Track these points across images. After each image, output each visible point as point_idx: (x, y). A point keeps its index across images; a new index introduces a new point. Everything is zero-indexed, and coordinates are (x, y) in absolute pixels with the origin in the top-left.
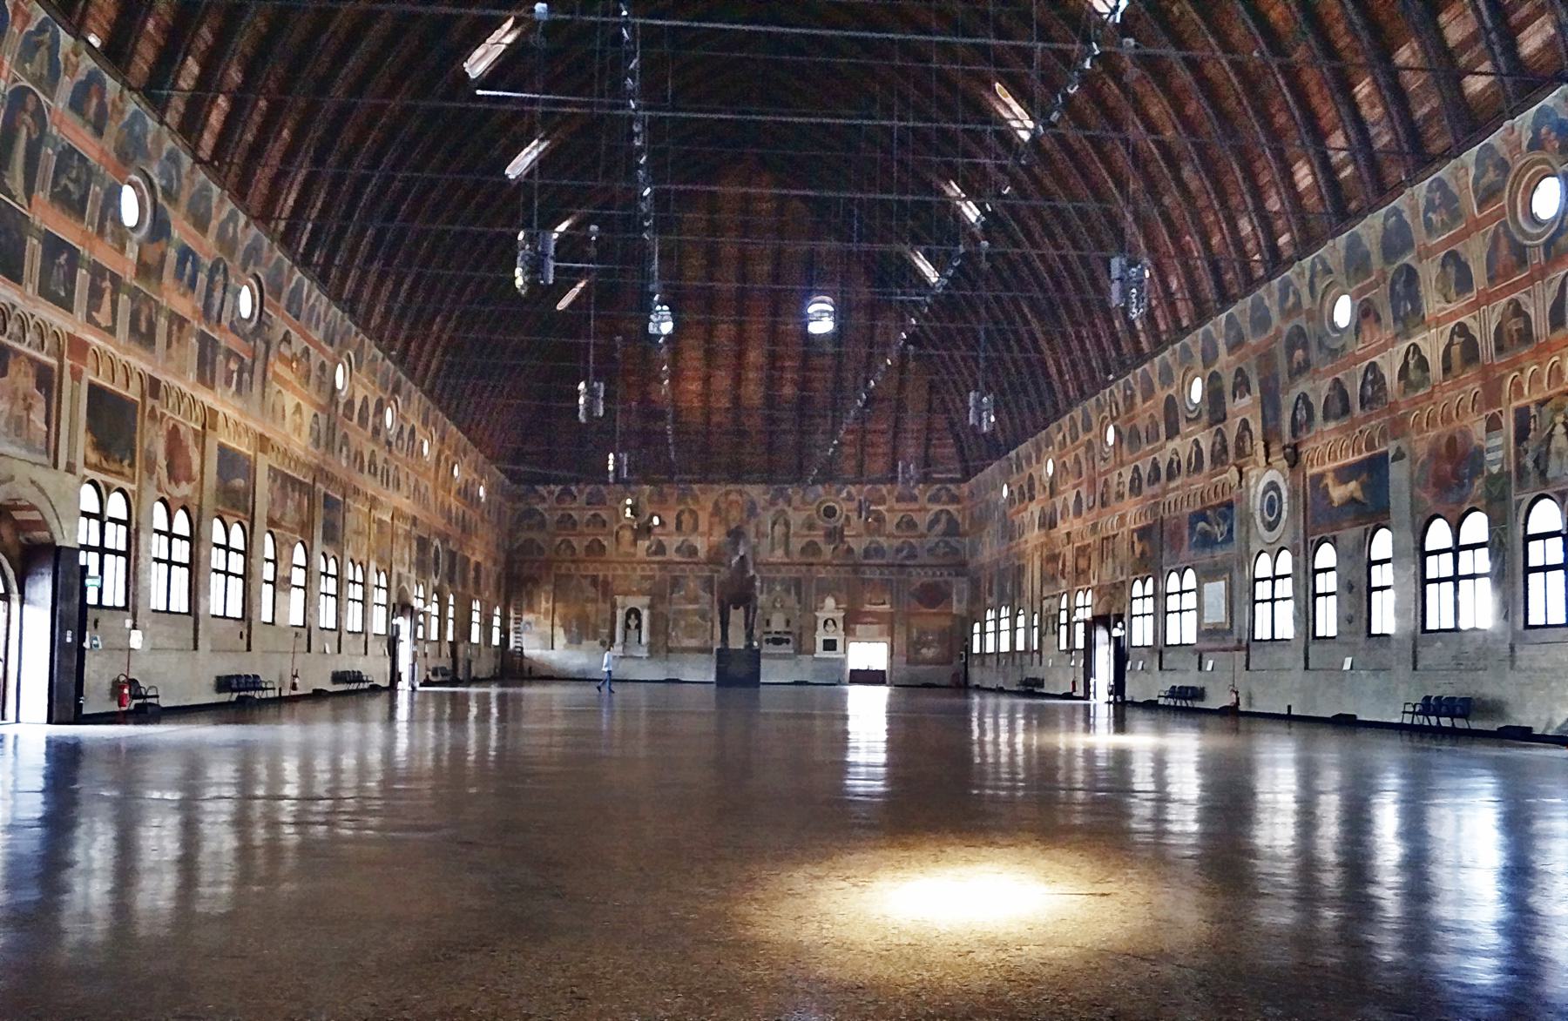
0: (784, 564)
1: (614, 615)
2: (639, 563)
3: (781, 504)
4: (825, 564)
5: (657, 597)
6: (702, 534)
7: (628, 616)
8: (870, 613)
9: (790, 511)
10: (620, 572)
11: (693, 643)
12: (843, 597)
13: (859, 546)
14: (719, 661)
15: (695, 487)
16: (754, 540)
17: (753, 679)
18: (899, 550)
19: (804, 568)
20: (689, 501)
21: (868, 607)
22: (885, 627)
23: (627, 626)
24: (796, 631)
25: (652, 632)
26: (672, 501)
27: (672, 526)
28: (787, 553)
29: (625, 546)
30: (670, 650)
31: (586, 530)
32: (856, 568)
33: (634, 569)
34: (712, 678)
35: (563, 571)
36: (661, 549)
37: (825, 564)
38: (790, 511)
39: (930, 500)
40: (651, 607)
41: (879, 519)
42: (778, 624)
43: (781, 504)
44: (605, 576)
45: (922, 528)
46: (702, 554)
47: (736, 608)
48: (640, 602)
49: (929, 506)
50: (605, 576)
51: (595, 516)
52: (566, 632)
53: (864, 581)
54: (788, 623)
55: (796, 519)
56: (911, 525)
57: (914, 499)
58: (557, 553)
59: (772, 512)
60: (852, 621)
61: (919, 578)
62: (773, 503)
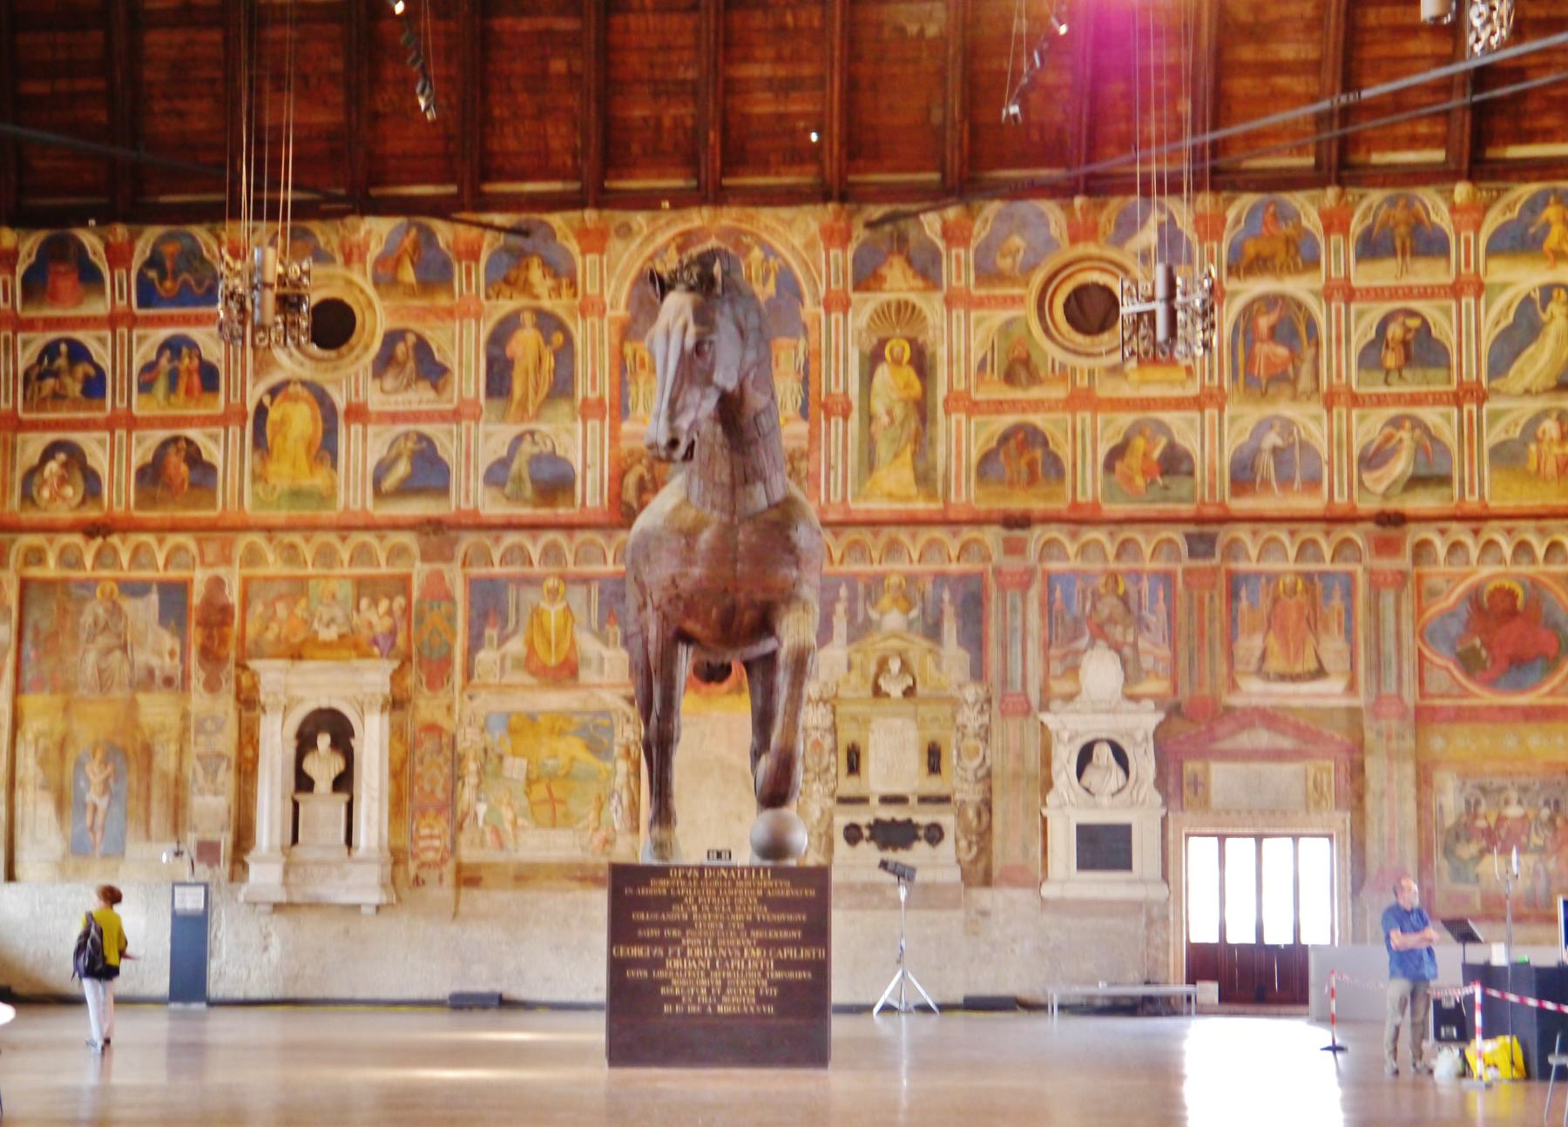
0: (913, 522)
1: (248, 739)
2: (344, 529)
3: (898, 282)
4: (1080, 518)
5: (420, 663)
6: (590, 410)
7: (305, 742)
8: (1269, 718)
9: (932, 307)
10: (273, 565)
11: (560, 846)
12: (1153, 648)
13: (1213, 441)
14: (621, 929)
15: (556, 220)
16: (792, 431)
17: (795, 1023)
18: (1373, 459)
19: (992, 537)
20: (536, 274)
21: (1254, 691)
22: (1327, 769)
23: (304, 783)
24: (969, 794)
25: (398, 805)
26: (470, 281)
27: (469, 379)
28: (924, 478)
29: (290, 466)
30: (468, 878)
31: (141, 407)
32: (1205, 531)
33: (326, 556)
34: (602, 996)
35: (51, 569)
36: (428, 471)
37: (1080, 518)
38: (932, 307)
39: (1493, 251)
40: (397, 703)
41: (1292, 326)
42: (893, 765)
43: (898, 282)
44: (217, 584)
45: (1471, 364)
46: (592, 493)
47: (713, 674)
48: (355, 687)
49: (1497, 271)
50: (217, 584)
51: (173, 347)
52: (60, 805)
53: (1234, 584)
54: (934, 759)
55: (962, 337)
56: (1422, 349)
57: (1430, 244)
58: (28, 497)
59: (866, 306)
60: (1190, 734)
61: (1465, 569)
62: (866, 279)
